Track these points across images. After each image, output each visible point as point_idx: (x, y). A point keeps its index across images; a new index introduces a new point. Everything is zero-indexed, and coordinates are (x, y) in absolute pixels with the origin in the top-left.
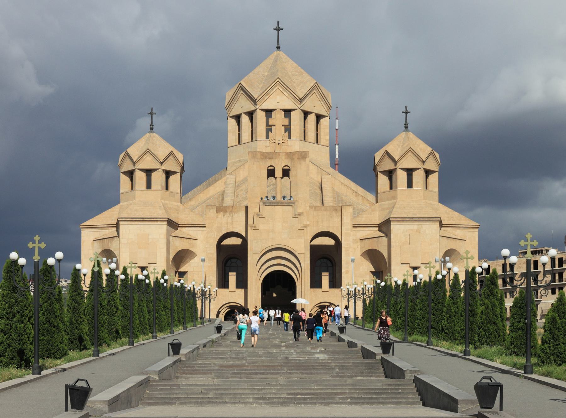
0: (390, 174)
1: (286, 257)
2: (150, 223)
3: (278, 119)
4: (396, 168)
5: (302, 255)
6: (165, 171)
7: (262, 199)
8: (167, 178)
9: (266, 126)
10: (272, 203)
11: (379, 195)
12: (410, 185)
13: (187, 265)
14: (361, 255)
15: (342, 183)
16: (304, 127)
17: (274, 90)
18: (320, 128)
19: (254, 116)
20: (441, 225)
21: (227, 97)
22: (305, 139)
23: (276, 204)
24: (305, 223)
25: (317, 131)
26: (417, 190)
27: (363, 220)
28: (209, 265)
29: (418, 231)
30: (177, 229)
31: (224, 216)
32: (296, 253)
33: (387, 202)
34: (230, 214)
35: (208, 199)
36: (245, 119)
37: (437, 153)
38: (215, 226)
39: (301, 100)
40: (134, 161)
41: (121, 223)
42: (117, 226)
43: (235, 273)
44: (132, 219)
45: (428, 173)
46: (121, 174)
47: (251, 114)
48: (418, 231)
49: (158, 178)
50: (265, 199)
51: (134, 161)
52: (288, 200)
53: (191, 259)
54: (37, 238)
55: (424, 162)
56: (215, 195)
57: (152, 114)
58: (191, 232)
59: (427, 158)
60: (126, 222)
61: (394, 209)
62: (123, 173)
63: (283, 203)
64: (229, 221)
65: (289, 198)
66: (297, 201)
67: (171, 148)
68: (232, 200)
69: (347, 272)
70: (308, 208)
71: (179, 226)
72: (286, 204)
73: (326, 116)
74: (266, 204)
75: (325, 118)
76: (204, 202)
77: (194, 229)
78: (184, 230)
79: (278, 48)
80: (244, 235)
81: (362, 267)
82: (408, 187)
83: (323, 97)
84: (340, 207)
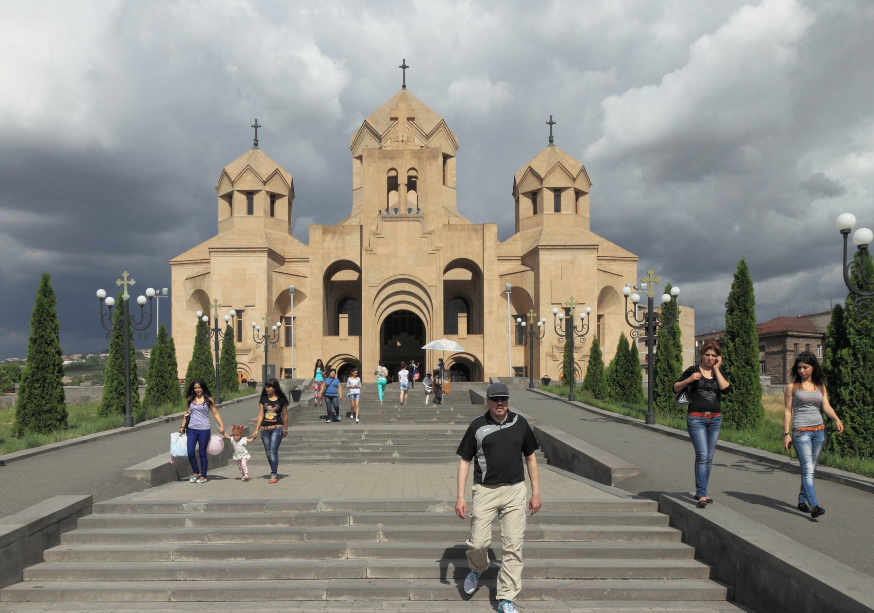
0: (534, 195)
1: (412, 291)
2: (246, 255)
6: (269, 194)
7: (380, 211)
8: (273, 203)
10: (394, 217)
11: (520, 221)
12: (557, 209)
18: (447, 169)
23: (399, 219)
24: (437, 245)
26: (567, 214)
30: (283, 265)
31: (333, 238)
33: (530, 230)
34: (340, 236)
38: (321, 252)
40: (232, 180)
44: (225, 250)
45: (578, 194)
46: (219, 198)
49: (261, 202)
50: (384, 213)
51: (232, 180)
52: (415, 215)
54: (125, 274)
61: (542, 237)
62: (220, 197)
63: (409, 217)
64: (339, 246)
65: (417, 211)
66: (426, 214)
71: (286, 260)
72: (412, 219)
73: (453, 157)
74: (386, 219)
75: (452, 159)
80: (359, 264)
83: (450, 136)
84: (482, 227)
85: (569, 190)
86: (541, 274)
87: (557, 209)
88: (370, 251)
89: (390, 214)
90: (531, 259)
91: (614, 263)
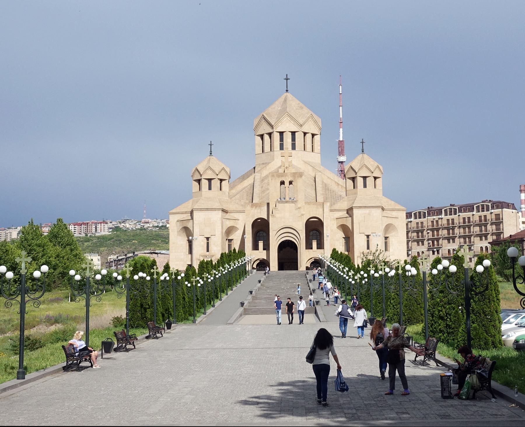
0: (353, 179)
2: (211, 211)
3: (288, 138)
5: (301, 231)
8: (221, 183)
9: (280, 142)
12: (365, 186)
13: (233, 235)
14: (337, 228)
15: (328, 177)
16: (304, 142)
17: (285, 119)
18: (314, 142)
19: (272, 135)
20: (383, 209)
21: (255, 122)
22: (304, 150)
24: (302, 213)
25: (312, 144)
27: (337, 206)
29: (369, 214)
35: (244, 189)
36: (266, 137)
37: (381, 165)
39: (301, 126)
41: (194, 212)
42: (192, 213)
43: (262, 242)
45: (375, 178)
47: (270, 134)
48: (369, 214)
49: (215, 184)
52: (293, 201)
53: (236, 232)
55: (372, 172)
56: (247, 187)
58: (236, 215)
59: (375, 170)
61: (355, 201)
67: (223, 166)
68: (258, 190)
69: (327, 240)
70: (304, 204)
76: (241, 191)
77: (238, 214)
78: (231, 214)
79: (287, 91)
83: (316, 122)
86: (354, 219)
88: (273, 216)
89: (282, 200)
90: (350, 211)
91: (394, 212)
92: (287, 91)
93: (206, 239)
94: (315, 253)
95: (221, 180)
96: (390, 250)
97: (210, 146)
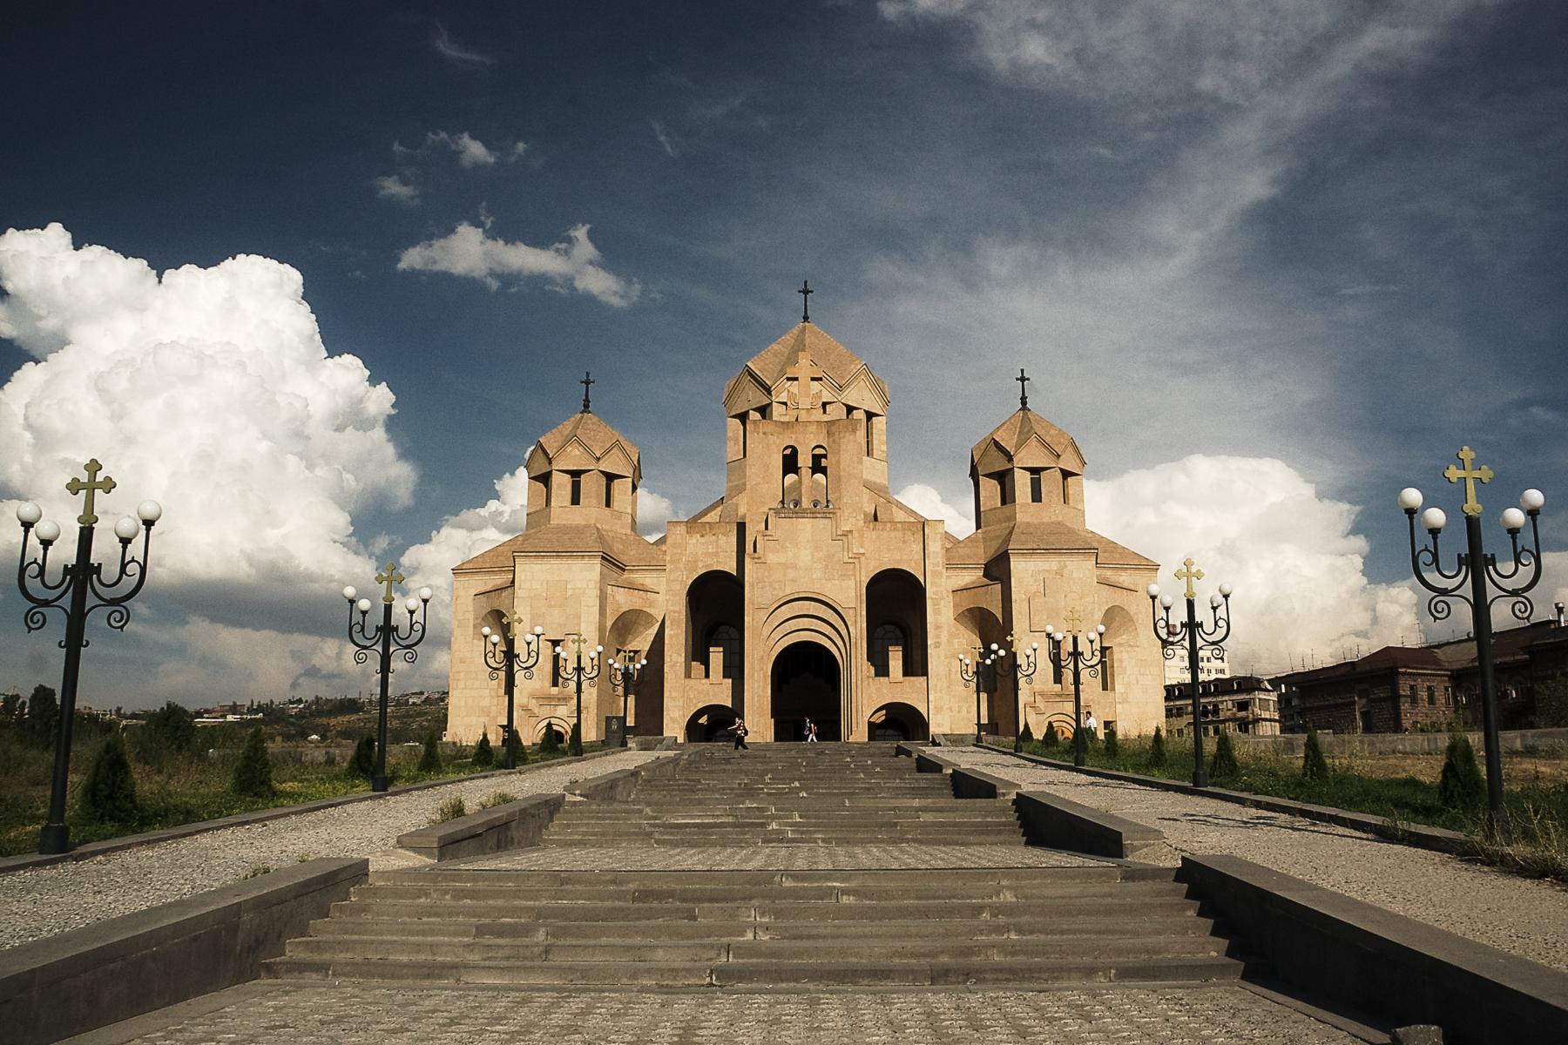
4: (1010, 466)
5: (851, 611)
11: (982, 514)
12: (1037, 496)
25: (868, 437)
28: (672, 632)
29: (1059, 573)
32: (839, 609)
40: (550, 456)
48: (1059, 573)
49: (592, 486)
52: (824, 508)
57: (587, 383)
60: (527, 560)
67: (617, 436)
69: (937, 645)
70: (861, 523)
72: (819, 516)
77: (654, 574)
79: (806, 318)
81: (956, 641)
82: (1033, 501)
85: (1053, 470)
87: (1037, 496)
88: (758, 560)
92: (806, 318)
93: (550, 643)
94: (897, 688)
95: (610, 478)
96: (1117, 687)
97: (584, 385)
